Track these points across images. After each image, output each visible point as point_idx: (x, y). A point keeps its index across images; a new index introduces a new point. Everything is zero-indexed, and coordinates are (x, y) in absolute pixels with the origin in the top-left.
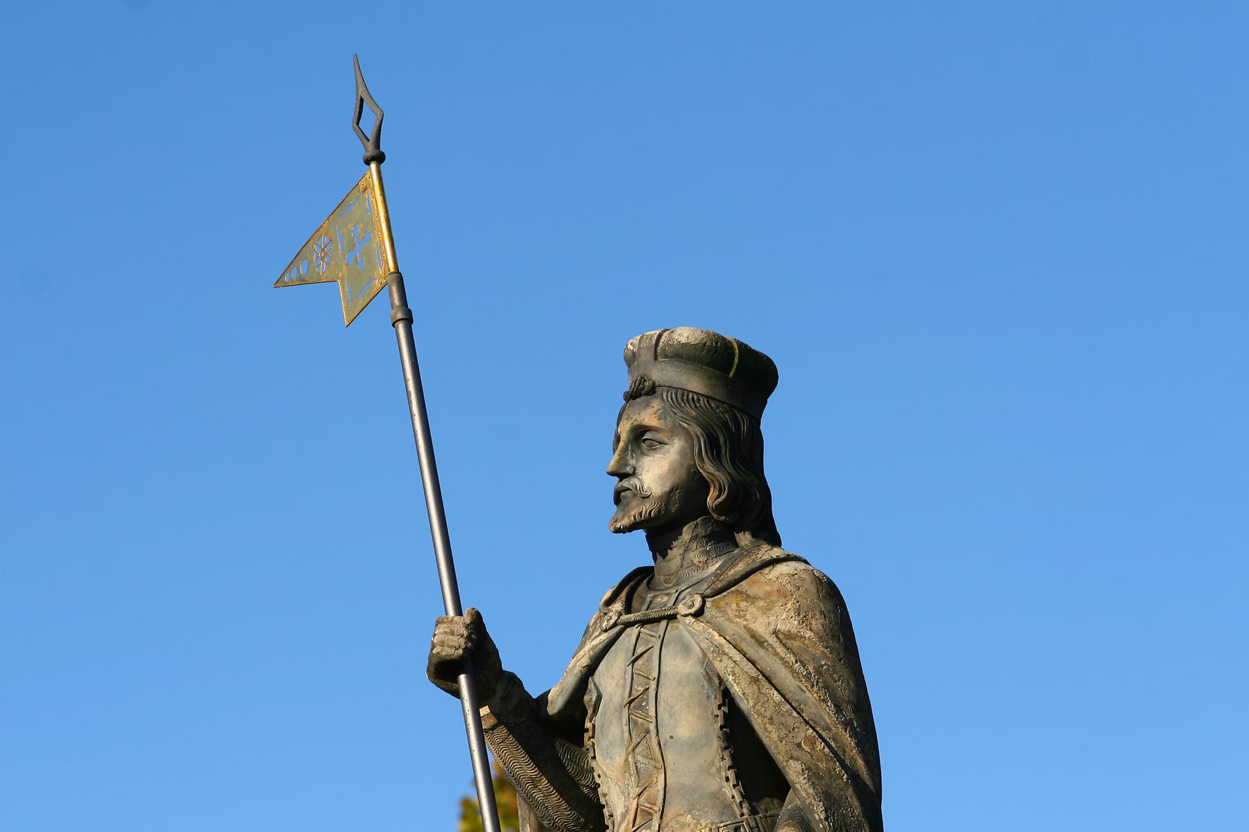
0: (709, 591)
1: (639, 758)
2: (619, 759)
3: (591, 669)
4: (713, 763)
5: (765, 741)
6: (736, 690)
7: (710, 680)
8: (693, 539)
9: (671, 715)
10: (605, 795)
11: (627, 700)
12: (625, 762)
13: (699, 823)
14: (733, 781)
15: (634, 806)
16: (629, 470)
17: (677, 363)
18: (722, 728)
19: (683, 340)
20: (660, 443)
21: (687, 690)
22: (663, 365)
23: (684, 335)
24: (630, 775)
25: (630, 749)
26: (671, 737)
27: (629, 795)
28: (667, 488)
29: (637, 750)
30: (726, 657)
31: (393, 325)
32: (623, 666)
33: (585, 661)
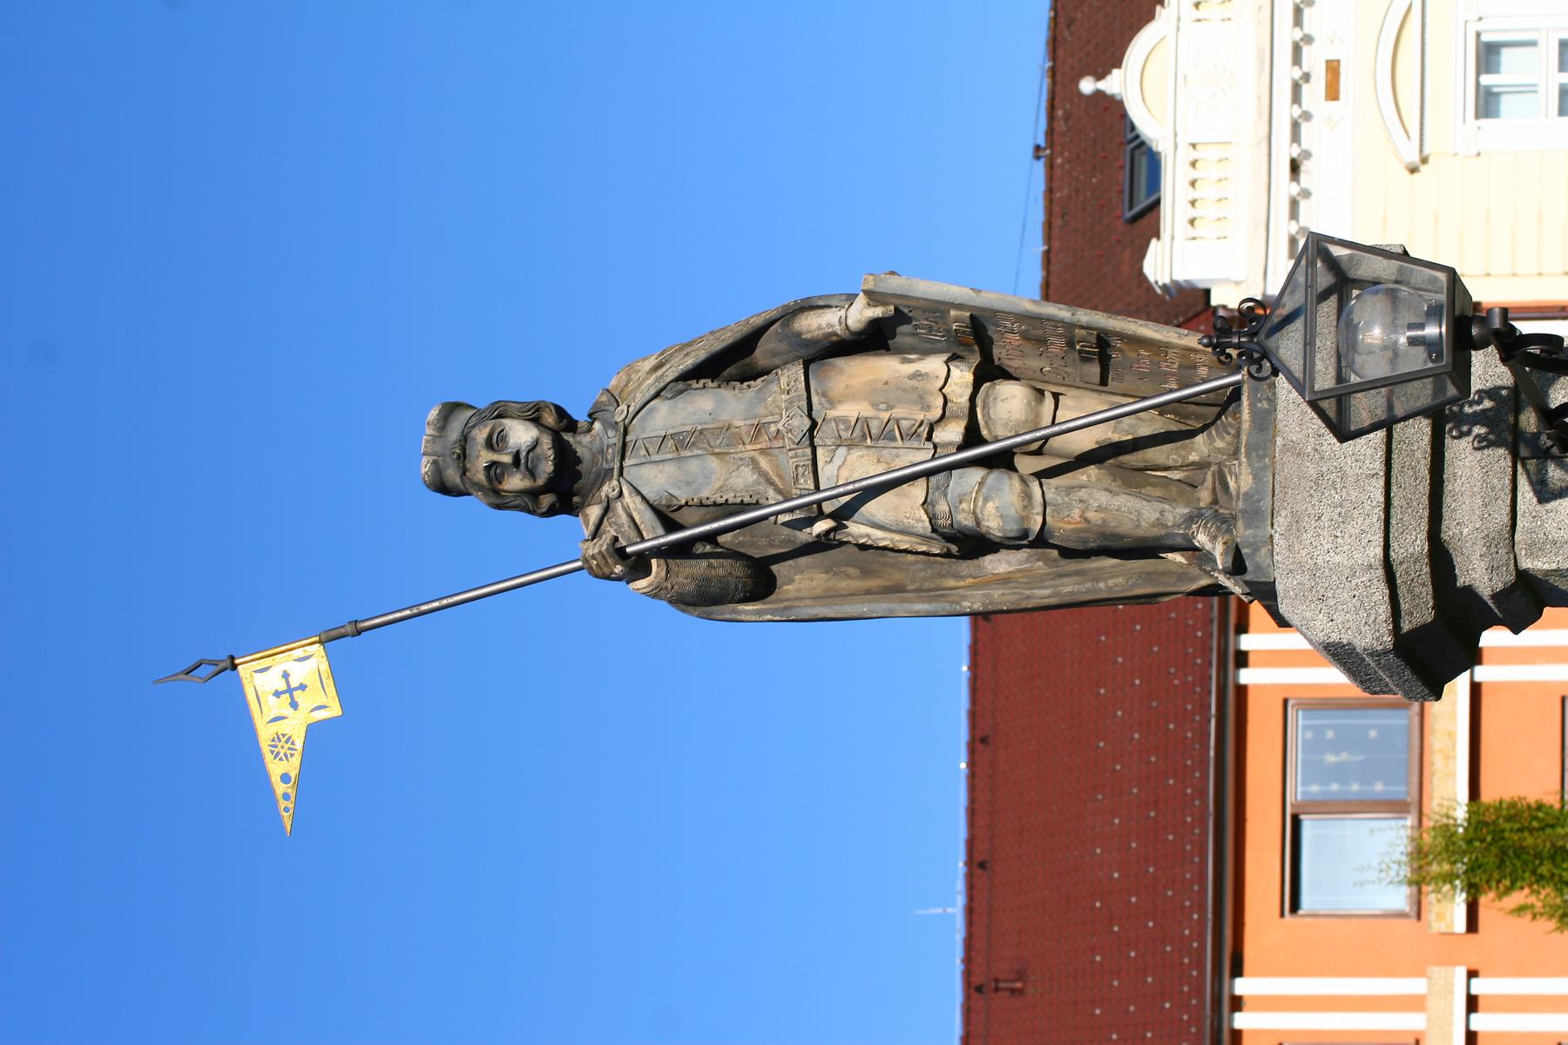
0: (615, 404)
1: (718, 442)
2: (713, 463)
3: (643, 498)
4: (735, 395)
5: (730, 341)
6: (689, 362)
7: (681, 392)
8: (574, 438)
9: (695, 414)
10: (735, 497)
11: (674, 455)
12: (717, 458)
13: (775, 392)
14: (752, 383)
15: (749, 447)
16: (515, 450)
17: (451, 419)
18: (713, 382)
19: (437, 412)
20: (503, 431)
21: (680, 405)
22: (449, 429)
23: (433, 413)
24: (728, 454)
25: (710, 449)
26: (710, 414)
27: (741, 459)
28: (536, 429)
29: (712, 444)
30: (665, 374)
31: (359, 633)
32: (649, 467)
33: (638, 499)
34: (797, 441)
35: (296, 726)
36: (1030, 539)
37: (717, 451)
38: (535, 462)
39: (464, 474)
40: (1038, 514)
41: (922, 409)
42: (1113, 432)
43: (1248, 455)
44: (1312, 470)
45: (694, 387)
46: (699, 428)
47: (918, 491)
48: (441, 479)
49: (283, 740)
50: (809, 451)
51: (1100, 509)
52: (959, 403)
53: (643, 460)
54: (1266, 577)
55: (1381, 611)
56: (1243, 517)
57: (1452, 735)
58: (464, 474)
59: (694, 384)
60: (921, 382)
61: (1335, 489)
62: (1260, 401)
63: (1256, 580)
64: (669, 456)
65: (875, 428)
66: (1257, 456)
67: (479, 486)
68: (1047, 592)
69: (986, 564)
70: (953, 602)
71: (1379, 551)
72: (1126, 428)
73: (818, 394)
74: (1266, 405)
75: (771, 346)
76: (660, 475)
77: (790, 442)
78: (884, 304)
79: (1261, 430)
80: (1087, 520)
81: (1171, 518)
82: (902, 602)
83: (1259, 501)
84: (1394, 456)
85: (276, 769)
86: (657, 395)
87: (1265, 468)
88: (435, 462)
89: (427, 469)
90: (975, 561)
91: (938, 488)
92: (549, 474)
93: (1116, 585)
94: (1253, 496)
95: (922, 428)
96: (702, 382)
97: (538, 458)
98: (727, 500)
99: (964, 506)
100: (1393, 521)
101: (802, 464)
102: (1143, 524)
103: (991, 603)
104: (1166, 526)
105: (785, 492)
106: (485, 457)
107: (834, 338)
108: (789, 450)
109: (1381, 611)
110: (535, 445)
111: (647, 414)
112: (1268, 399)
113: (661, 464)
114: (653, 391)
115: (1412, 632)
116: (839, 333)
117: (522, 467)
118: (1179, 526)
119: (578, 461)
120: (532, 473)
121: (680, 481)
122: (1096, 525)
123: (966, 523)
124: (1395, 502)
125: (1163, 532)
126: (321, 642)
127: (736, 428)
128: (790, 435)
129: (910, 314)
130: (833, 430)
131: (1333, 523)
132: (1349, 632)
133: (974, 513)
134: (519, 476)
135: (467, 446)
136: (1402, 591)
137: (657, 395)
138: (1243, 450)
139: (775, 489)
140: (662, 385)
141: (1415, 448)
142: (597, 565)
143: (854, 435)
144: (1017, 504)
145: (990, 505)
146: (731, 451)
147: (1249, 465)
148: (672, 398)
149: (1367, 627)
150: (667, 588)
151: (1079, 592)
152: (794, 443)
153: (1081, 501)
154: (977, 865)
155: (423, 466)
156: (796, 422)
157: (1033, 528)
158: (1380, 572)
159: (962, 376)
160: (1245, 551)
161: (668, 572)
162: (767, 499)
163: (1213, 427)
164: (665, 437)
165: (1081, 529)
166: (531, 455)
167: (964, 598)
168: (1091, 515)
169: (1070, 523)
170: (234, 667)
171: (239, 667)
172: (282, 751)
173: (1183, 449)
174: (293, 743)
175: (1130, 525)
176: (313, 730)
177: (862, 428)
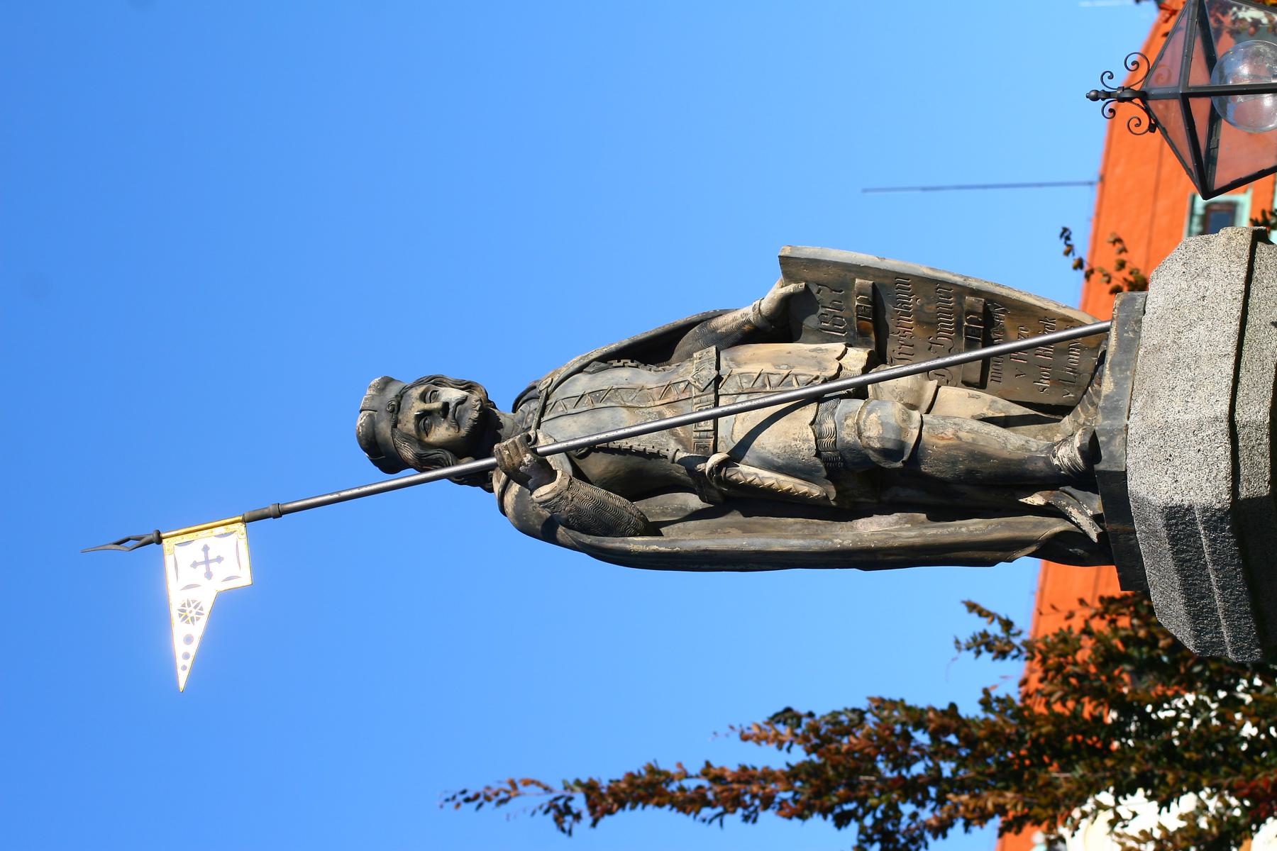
1: (630, 399)
2: (624, 413)
18: (632, 362)
20: (436, 391)
22: (388, 390)
27: (649, 413)
29: (625, 400)
32: (564, 418)
34: (702, 388)
36: (905, 458)
37: (629, 404)
38: (462, 413)
39: (395, 426)
40: (915, 428)
41: (819, 370)
42: (988, 409)
43: (1111, 369)
44: (1169, 356)
45: (614, 365)
46: (615, 387)
47: (809, 412)
48: (374, 431)
49: (193, 605)
50: (712, 396)
51: (971, 431)
52: (853, 371)
53: (562, 414)
54: (1118, 467)
55: (1222, 467)
56: (1102, 411)
58: (395, 426)
59: (615, 363)
60: (820, 355)
61: (1190, 369)
62: (1127, 332)
63: (1109, 469)
64: (585, 409)
65: (775, 379)
66: (1120, 370)
68: (913, 534)
69: (859, 525)
70: (825, 539)
71: (1226, 408)
72: (1001, 407)
73: (726, 360)
74: (1131, 335)
75: (688, 347)
76: (574, 424)
77: (697, 390)
78: (796, 282)
79: (1125, 352)
80: (958, 438)
81: (1036, 446)
82: (779, 537)
83: (1118, 401)
84: (1245, 348)
85: (180, 630)
86: (580, 370)
87: (1126, 378)
88: (370, 415)
89: (363, 420)
90: (849, 523)
91: (827, 410)
92: (474, 421)
93: (976, 530)
94: (1113, 397)
95: (817, 381)
96: (622, 361)
97: (466, 410)
98: (631, 447)
99: (849, 422)
100: (1240, 394)
101: (704, 408)
102: (1009, 446)
103: (861, 541)
104: (1030, 451)
105: (685, 440)
106: (417, 407)
107: (747, 327)
108: (695, 397)
109: (1222, 467)
110: (462, 402)
111: (570, 382)
112: (1134, 331)
113: (576, 416)
114: (577, 366)
115: (1248, 500)
116: (752, 320)
117: (450, 416)
118: (1042, 452)
119: (501, 426)
120: (457, 423)
121: (591, 428)
122: (967, 443)
123: (849, 439)
124: (1243, 381)
125: (1027, 455)
126: (245, 521)
127: (649, 389)
128: (697, 384)
129: (818, 296)
130: (737, 383)
131: (1185, 392)
132: (1192, 493)
133: (857, 423)
134: (445, 425)
135: (402, 403)
136: (1243, 455)
137: (580, 370)
138: (1107, 366)
139: (676, 440)
140: (586, 361)
141: (1265, 347)
142: (509, 455)
143: (755, 386)
144: (897, 416)
145: (873, 416)
146: (641, 406)
147: (1112, 376)
148: (593, 372)
149: (1208, 484)
150: (567, 498)
151: (942, 534)
152: (700, 390)
153: (955, 424)
155: (359, 419)
156: (704, 373)
157: (909, 442)
158: (1225, 425)
159: (857, 357)
160: (1101, 439)
161: (570, 482)
162: (668, 450)
163: (1079, 405)
164: (583, 396)
165: (952, 445)
166: (459, 406)
167: (837, 536)
168: (962, 434)
169: (943, 438)
170: (159, 540)
171: (164, 541)
172: (192, 608)
173: (1049, 430)
174: (201, 609)
175: (997, 446)
177: (764, 380)
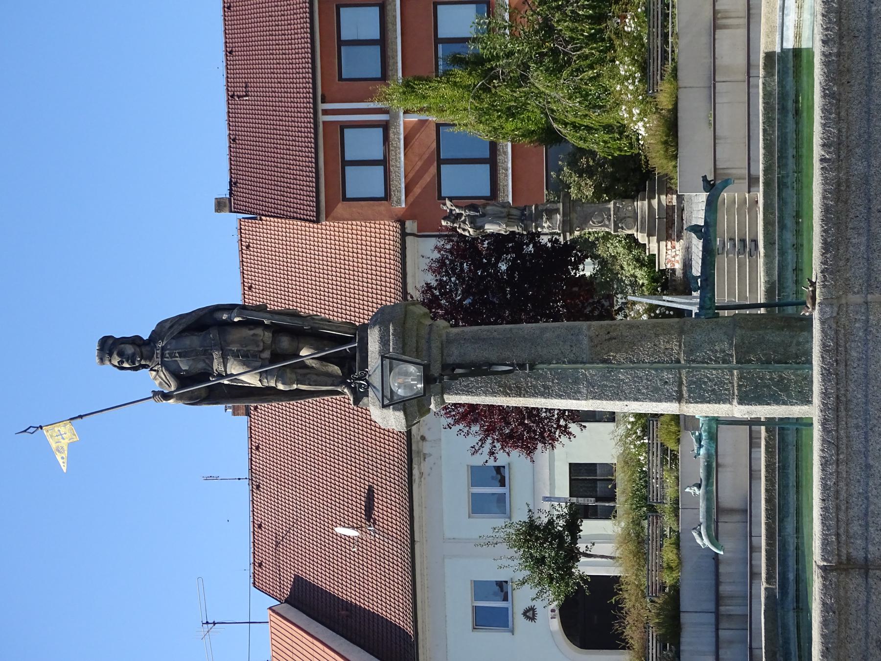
6: (181, 327)
35: (64, 443)
57: (395, 17)
67: (115, 366)
85: (59, 457)
154: (229, 53)
176: (70, 445)
